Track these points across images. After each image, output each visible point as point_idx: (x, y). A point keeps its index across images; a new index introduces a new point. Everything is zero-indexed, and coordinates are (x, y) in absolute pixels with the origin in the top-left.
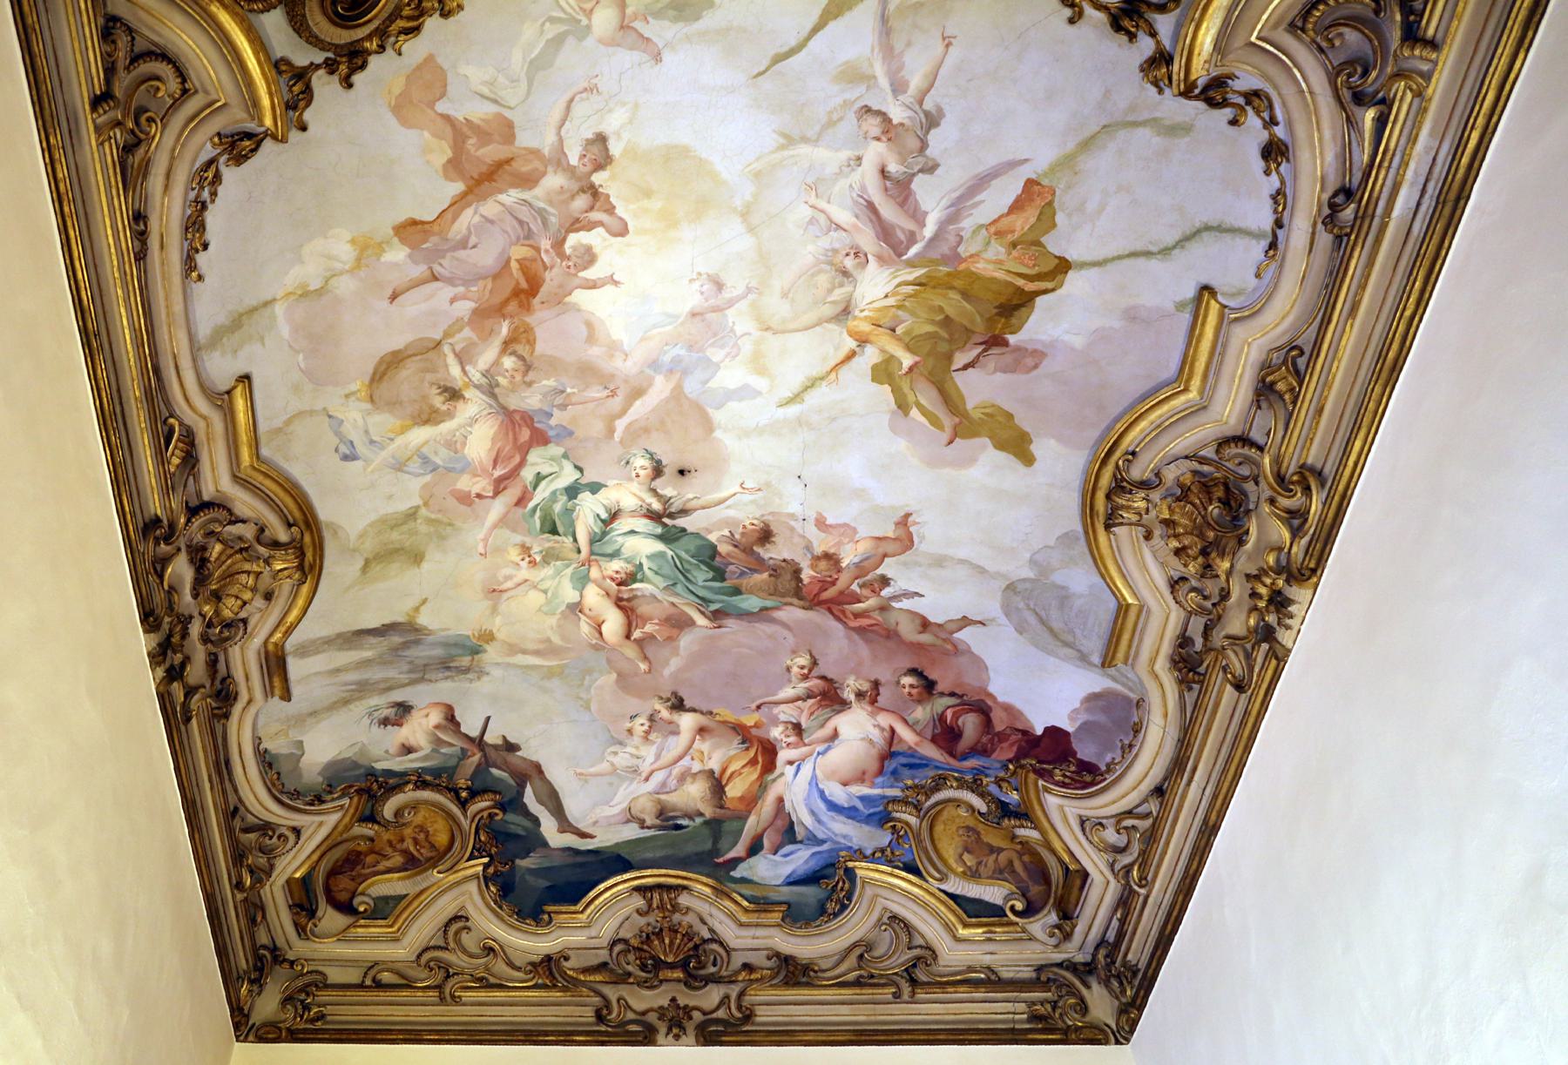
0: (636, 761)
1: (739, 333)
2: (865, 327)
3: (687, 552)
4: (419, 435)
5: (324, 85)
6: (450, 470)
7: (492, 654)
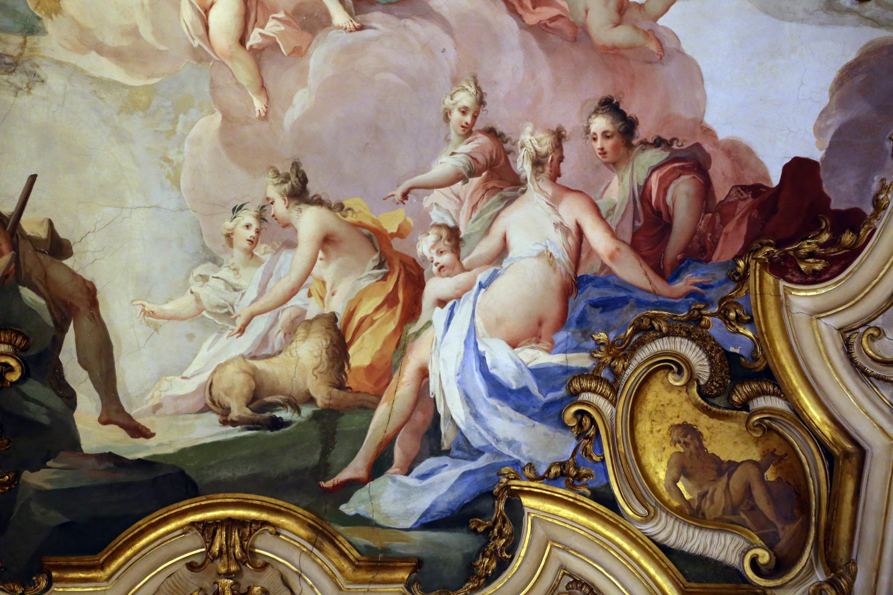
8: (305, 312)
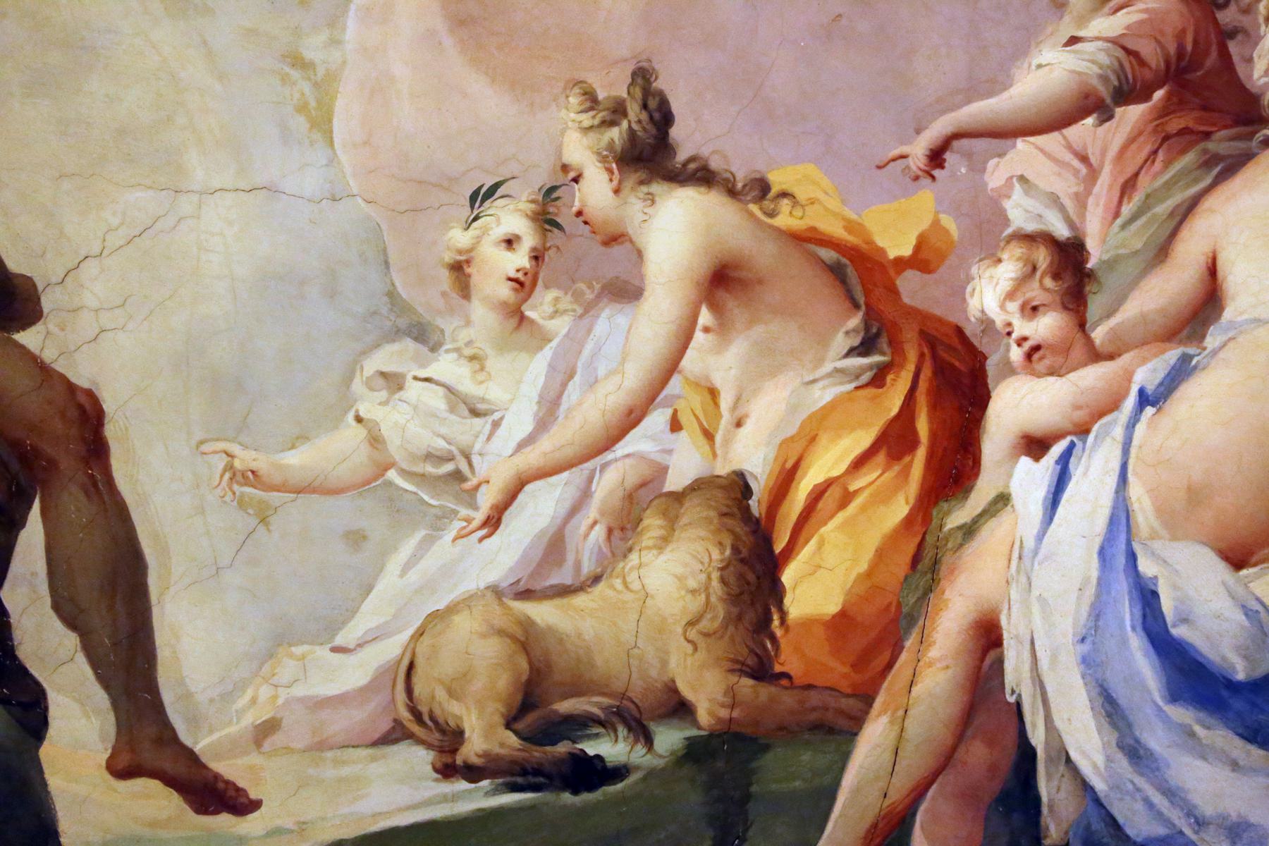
0: (465, 430)
8: (663, 470)
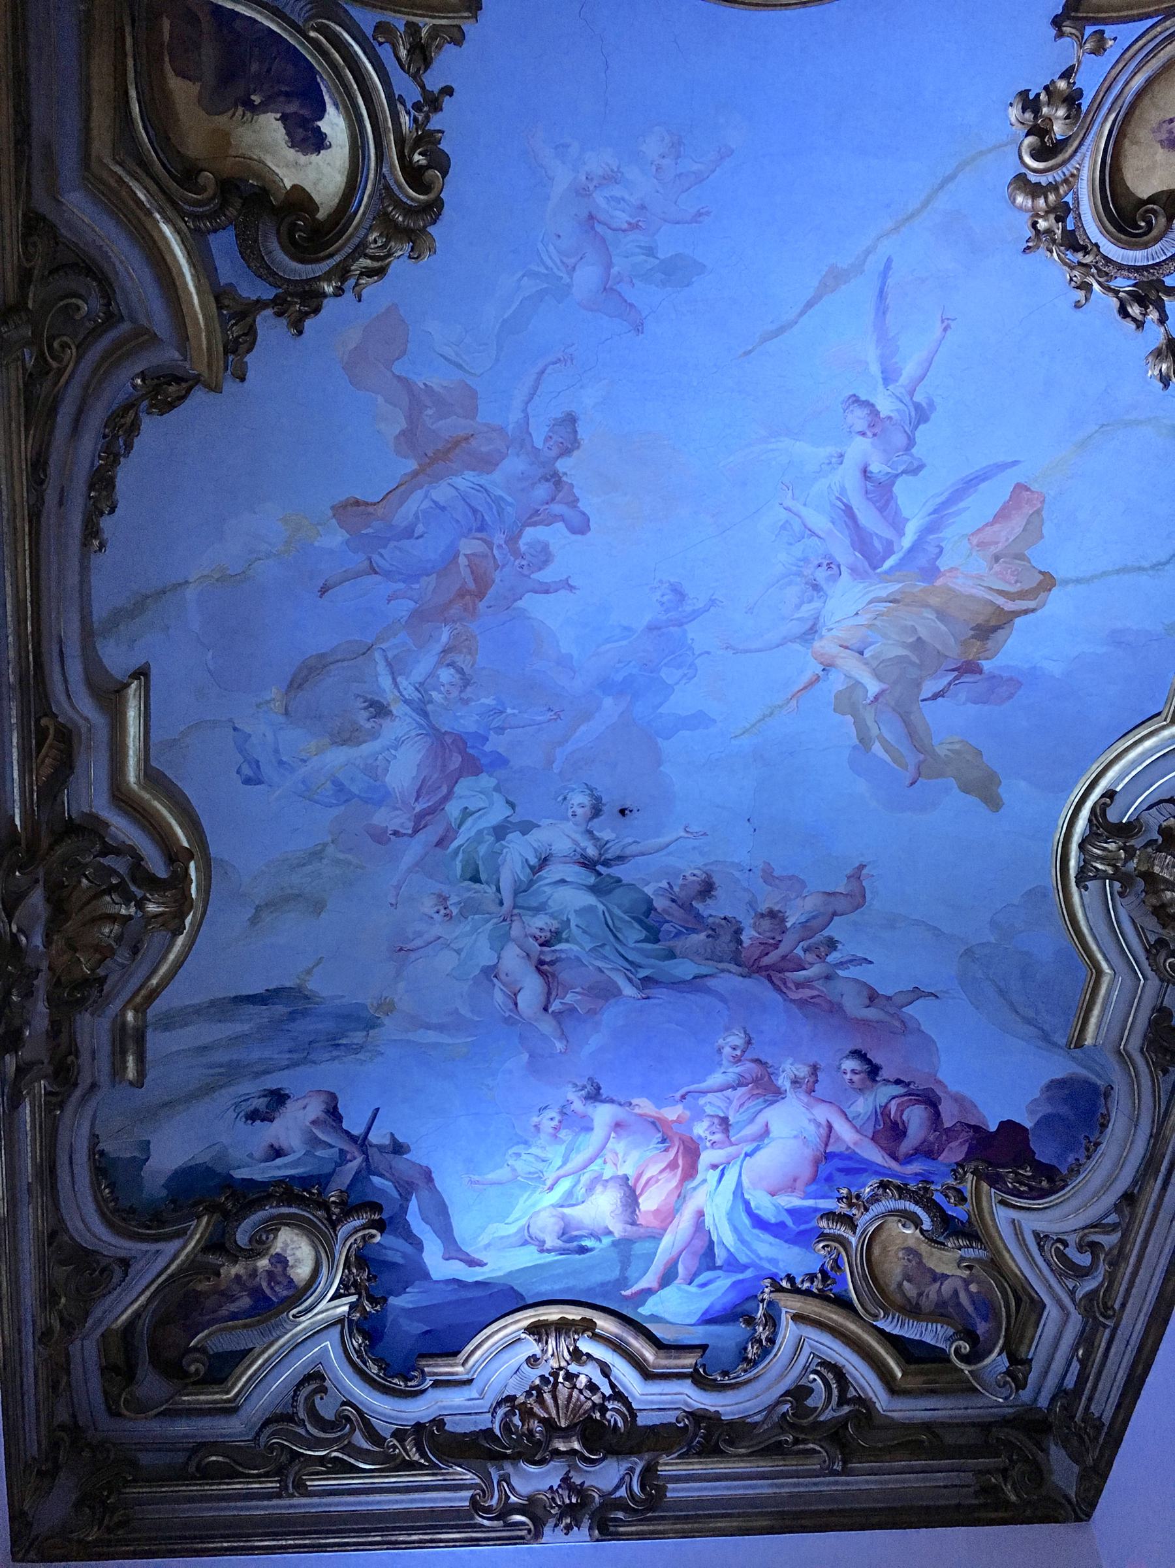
0: (541, 1166)
1: (697, 653)
2: (833, 649)
3: (619, 906)
4: (337, 758)
5: (269, 326)
6: (366, 801)
7: (390, 1028)
8: (602, 1175)
